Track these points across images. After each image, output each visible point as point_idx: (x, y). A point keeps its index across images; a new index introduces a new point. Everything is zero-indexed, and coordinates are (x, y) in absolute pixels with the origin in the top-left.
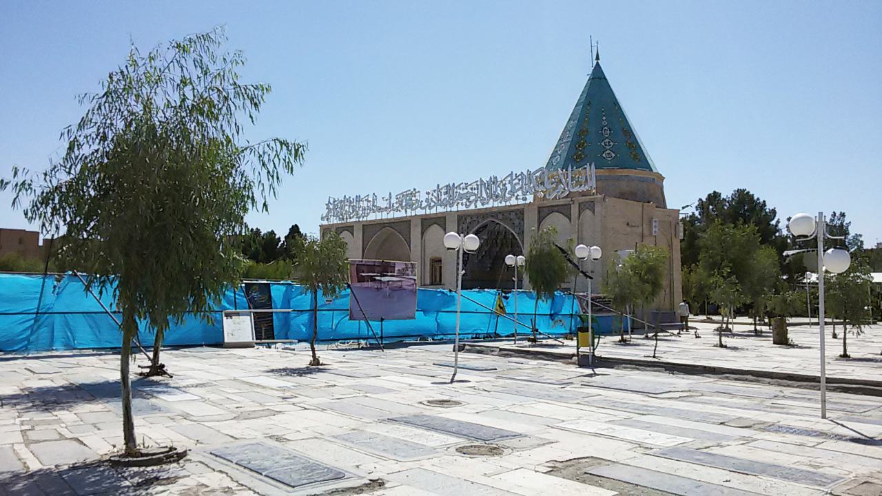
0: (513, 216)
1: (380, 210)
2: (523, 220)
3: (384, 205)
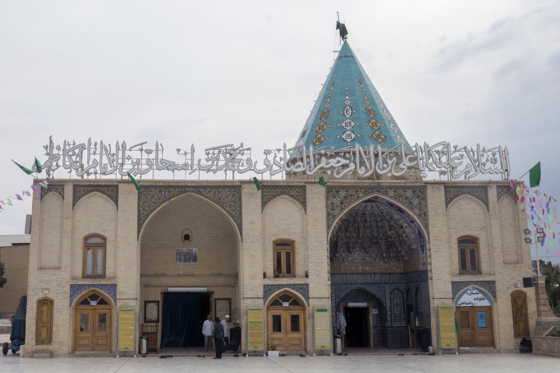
0: (409, 193)
3: (180, 160)
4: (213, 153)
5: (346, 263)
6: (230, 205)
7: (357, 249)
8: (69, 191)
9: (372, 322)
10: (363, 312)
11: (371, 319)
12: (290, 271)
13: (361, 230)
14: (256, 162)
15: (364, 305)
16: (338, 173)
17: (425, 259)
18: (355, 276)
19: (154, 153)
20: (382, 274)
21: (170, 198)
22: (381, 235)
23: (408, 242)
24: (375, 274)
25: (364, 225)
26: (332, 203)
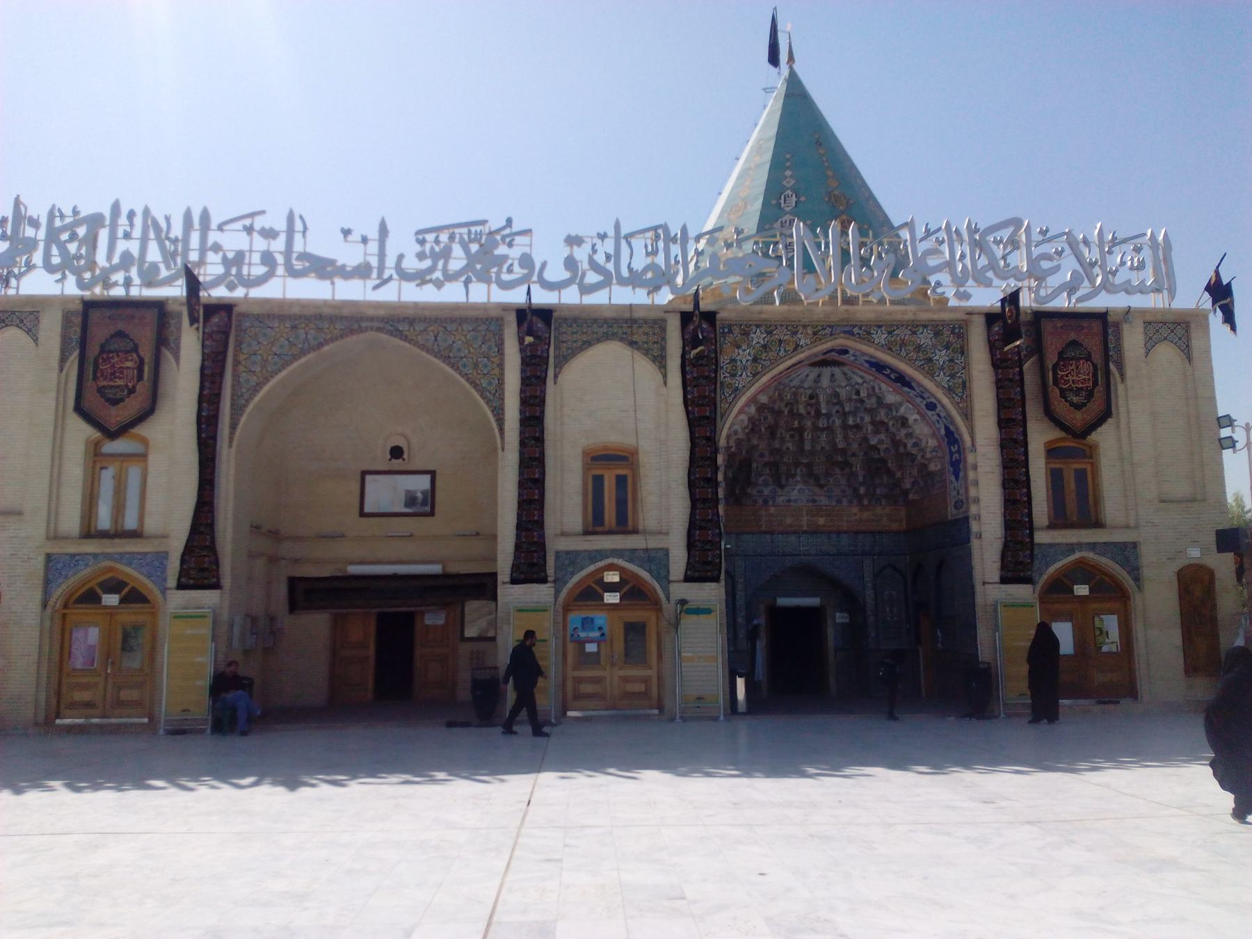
0: (925, 338)
1: (323, 268)
3: (350, 256)
4: (435, 243)
5: (772, 510)
6: (476, 365)
7: (798, 478)
9: (831, 637)
10: (813, 617)
11: (830, 633)
12: (624, 525)
13: (808, 436)
14: (544, 265)
15: (814, 601)
17: (962, 491)
18: (793, 538)
19: (282, 238)
20: (856, 533)
21: (320, 345)
22: (855, 446)
23: (919, 457)
24: (838, 533)
25: (813, 424)
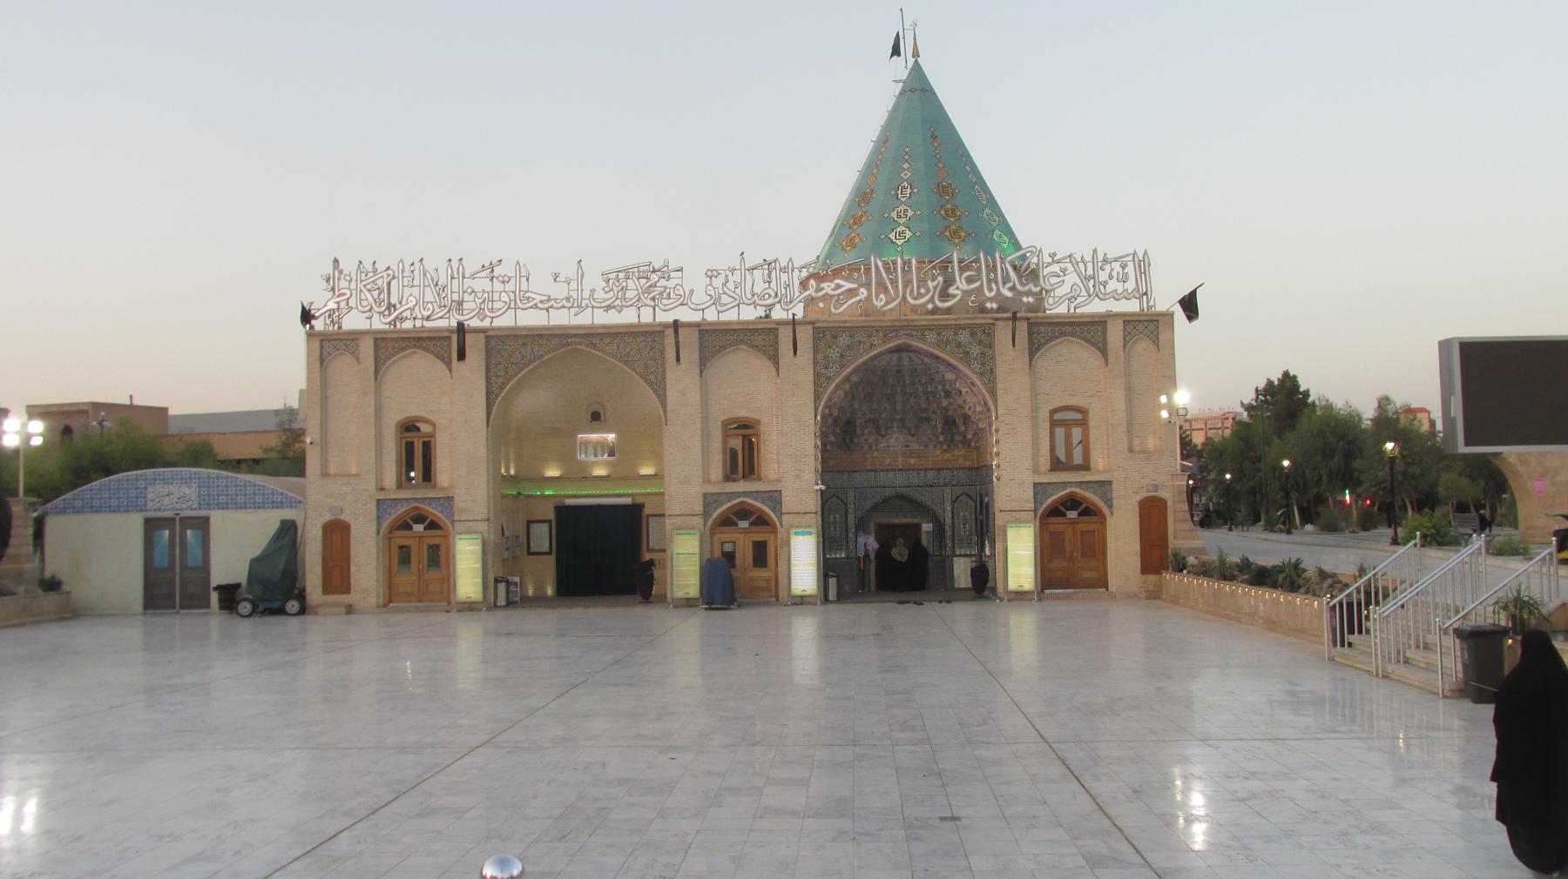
0: (964, 337)
2: (991, 346)
8: (367, 348)
16: (839, 304)
18: (891, 474)
26: (826, 357)
